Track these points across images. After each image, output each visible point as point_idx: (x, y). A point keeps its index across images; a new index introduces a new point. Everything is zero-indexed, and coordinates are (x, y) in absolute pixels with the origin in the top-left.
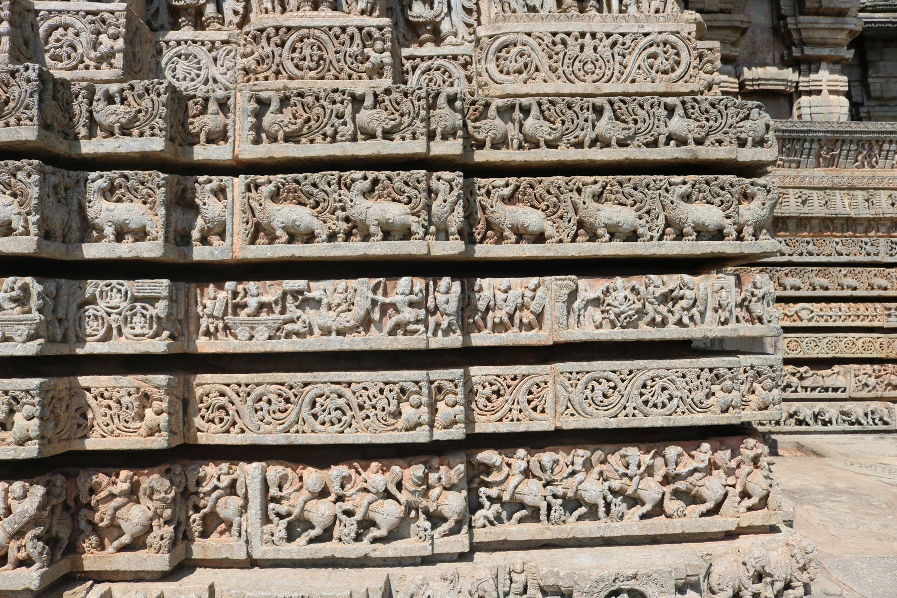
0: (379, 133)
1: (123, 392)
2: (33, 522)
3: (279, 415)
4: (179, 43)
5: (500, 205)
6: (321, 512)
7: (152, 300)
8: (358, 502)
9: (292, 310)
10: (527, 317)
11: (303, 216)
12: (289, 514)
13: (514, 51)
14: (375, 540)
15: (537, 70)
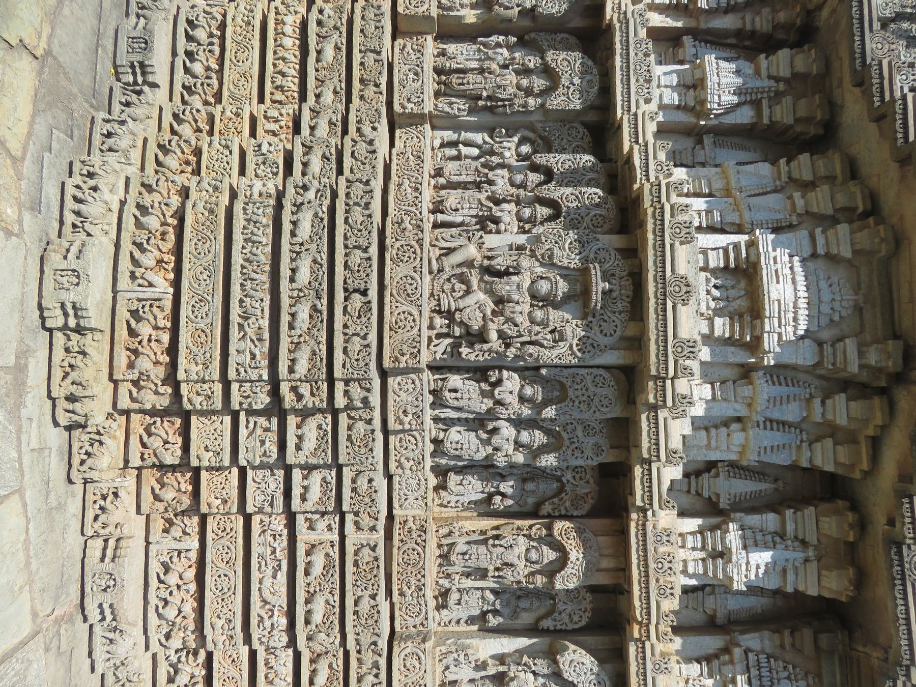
0: (357, 609)
1: (228, 491)
2: (160, 461)
3: (220, 558)
4: (426, 480)
5: (328, 663)
6: (173, 579)
7: (271, 505)
8: (176, 599)
9: (272, 564)
10: (271, 676)
11: (317, 570)
12: (172, 562)
13: (416, 663)
14: (157, 607)
15: (406, 676)
